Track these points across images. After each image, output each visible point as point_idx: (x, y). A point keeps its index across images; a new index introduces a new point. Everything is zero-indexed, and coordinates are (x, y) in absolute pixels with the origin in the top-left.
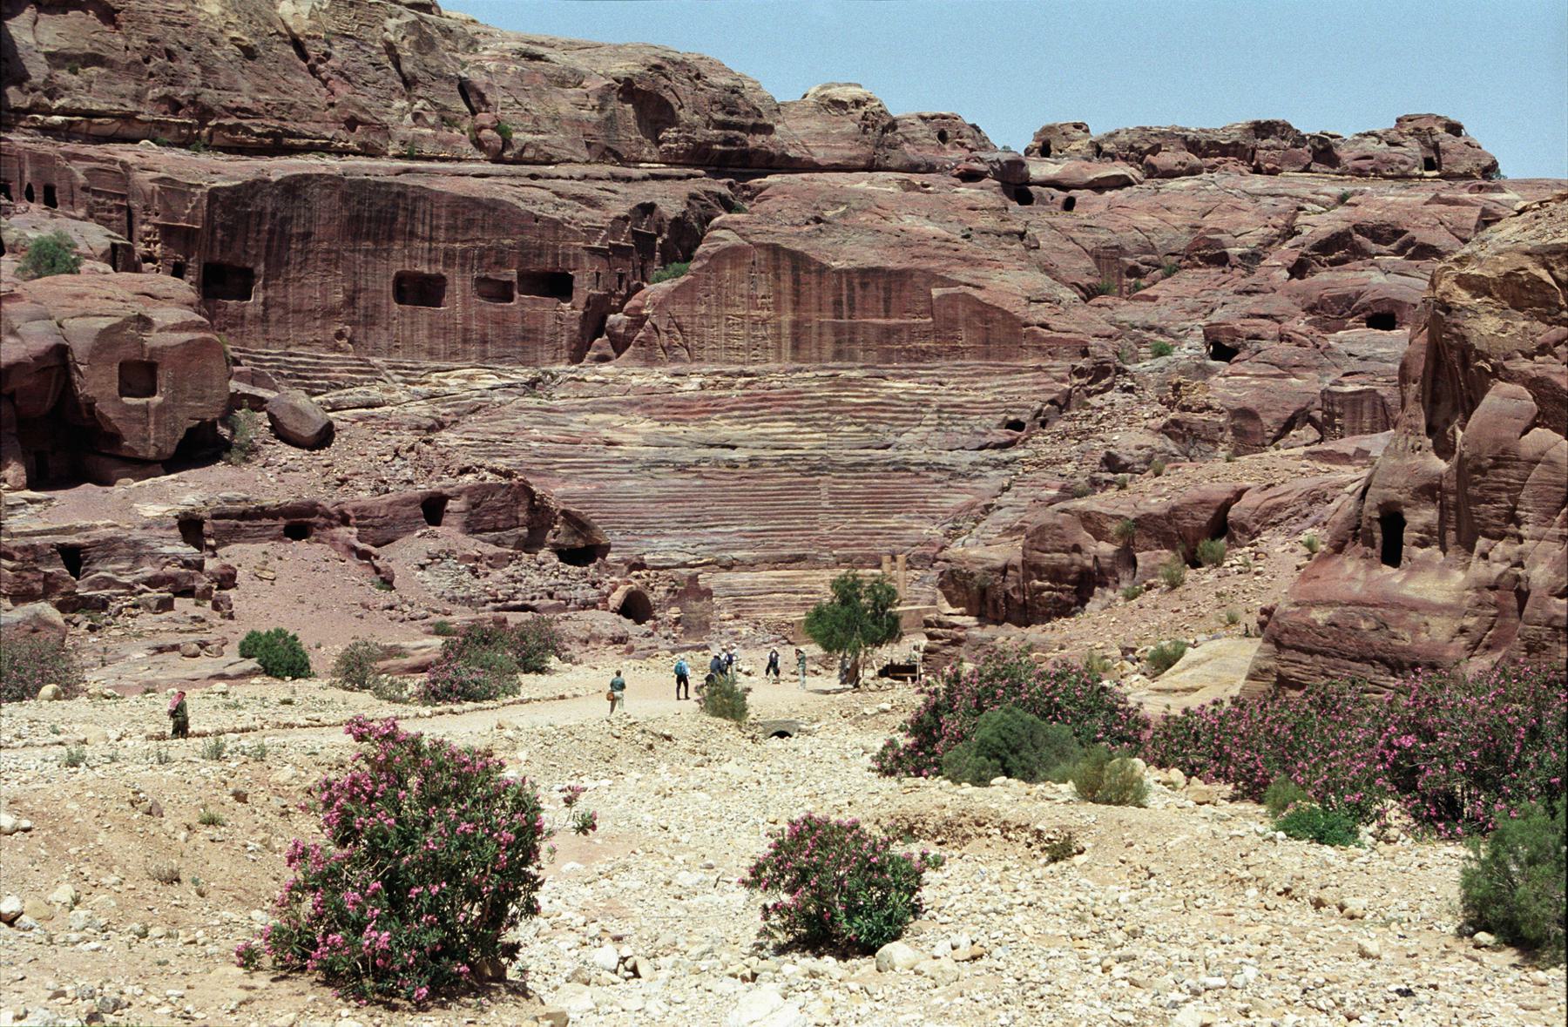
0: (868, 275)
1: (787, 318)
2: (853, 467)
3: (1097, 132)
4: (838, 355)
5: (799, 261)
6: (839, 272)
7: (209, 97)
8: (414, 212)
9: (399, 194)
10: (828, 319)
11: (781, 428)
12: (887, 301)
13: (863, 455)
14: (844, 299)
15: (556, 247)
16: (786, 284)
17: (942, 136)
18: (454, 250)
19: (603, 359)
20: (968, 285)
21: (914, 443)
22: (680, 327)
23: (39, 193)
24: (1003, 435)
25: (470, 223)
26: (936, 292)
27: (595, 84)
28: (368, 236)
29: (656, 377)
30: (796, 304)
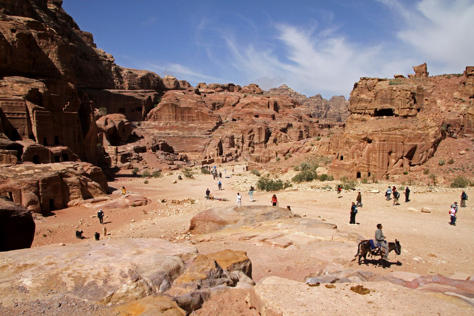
0: (186, 108)
1: (174, 114)
2: (188, 137)
3: (208, 84)
4: (182, 120)
5: (176, 106)
10: (180, 114)
11: (176, 131)
13: (189, 135)
16: (174, 109)
17: (184, 84)
19: (147, 120)
21: (196, 133)
24: (209, 133)
26: (196, 111)
27: (139, 77)
29: (156, 123)
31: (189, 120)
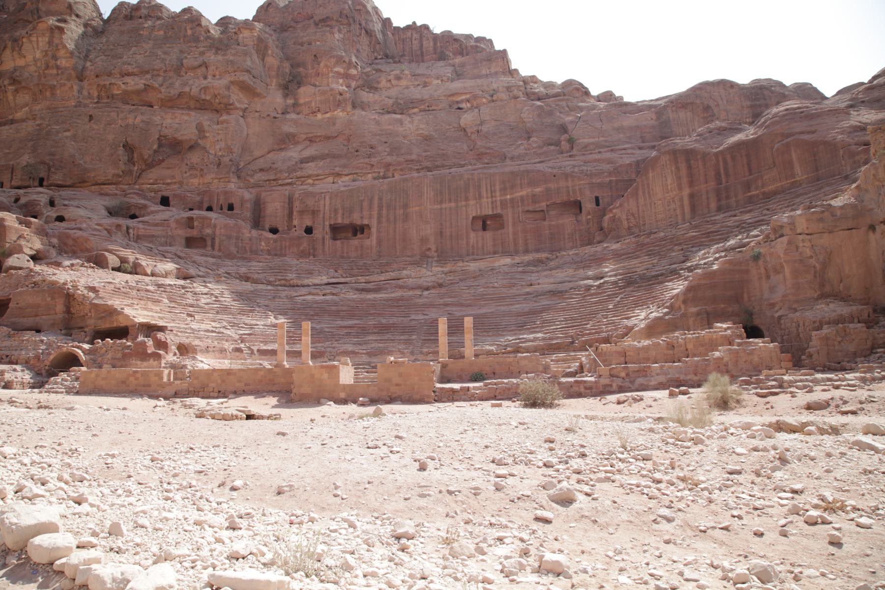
1: (686, 192)
4: (719, 209)
5: (689, 154)
6: (717, 155)
7: (389, 159)
8: (479, 186)
9: (468, 179)
10: (712, 184)
12: (749, 164)
14: (722, 171)
15: (568, 187)
16: (684, 172)
18: (506, 200)
20: (802, 133)
22: (633, 215)
23: (225, 207)
25: (513, 187)
28: (450, 201)
30: (691, 184)
31: (750, 200)
